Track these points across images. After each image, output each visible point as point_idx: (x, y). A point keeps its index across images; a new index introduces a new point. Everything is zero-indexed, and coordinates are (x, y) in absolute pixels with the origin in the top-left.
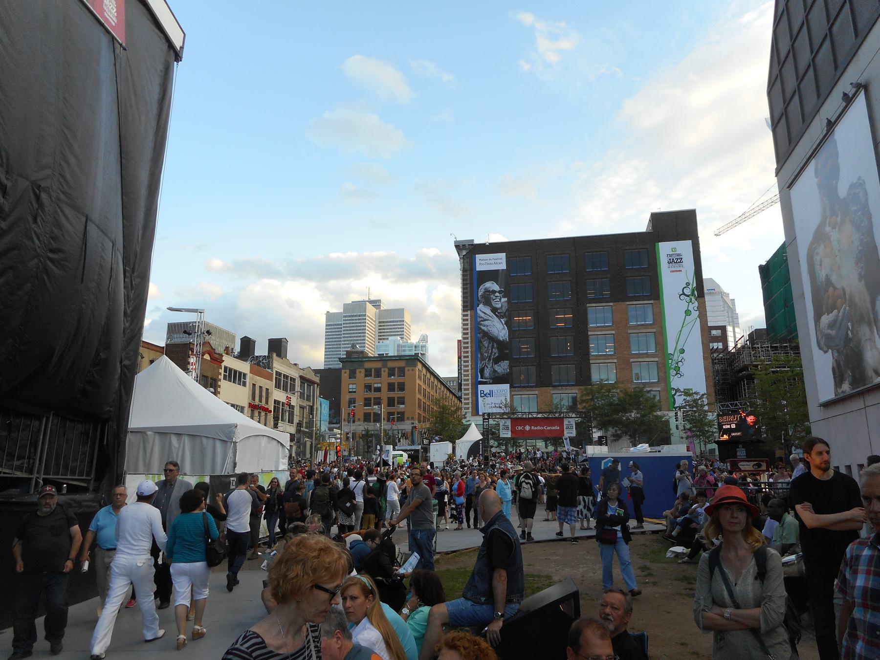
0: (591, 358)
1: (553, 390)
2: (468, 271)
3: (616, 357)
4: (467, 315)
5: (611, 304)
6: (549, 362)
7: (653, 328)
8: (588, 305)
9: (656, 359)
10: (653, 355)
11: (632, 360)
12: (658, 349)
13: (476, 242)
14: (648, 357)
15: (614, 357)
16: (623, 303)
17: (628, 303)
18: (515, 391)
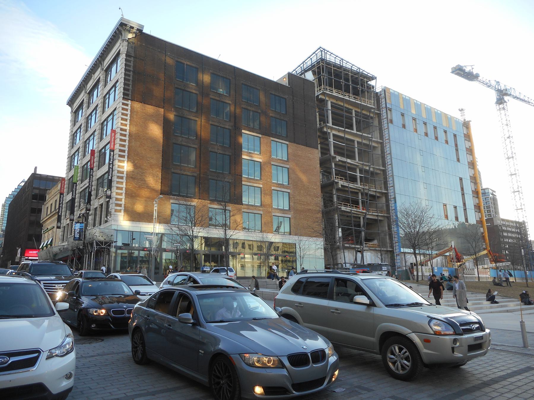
0: (243, 179)
1: (210, 204)
2: (132, 58)
3: (262, 183)
4: (127, 105)
5: (260, 136)
6: (208, 175)
7: (288, 164)
8: (243, 131)
9: (289, 191)
10: (286, 187)
11: (273, 188)
12: (290, 182)
13: (145, 31)
14: (283, 188)
15: (260, 182)
16: (268, 137)
17: (272, 138)
18: (174, 199)
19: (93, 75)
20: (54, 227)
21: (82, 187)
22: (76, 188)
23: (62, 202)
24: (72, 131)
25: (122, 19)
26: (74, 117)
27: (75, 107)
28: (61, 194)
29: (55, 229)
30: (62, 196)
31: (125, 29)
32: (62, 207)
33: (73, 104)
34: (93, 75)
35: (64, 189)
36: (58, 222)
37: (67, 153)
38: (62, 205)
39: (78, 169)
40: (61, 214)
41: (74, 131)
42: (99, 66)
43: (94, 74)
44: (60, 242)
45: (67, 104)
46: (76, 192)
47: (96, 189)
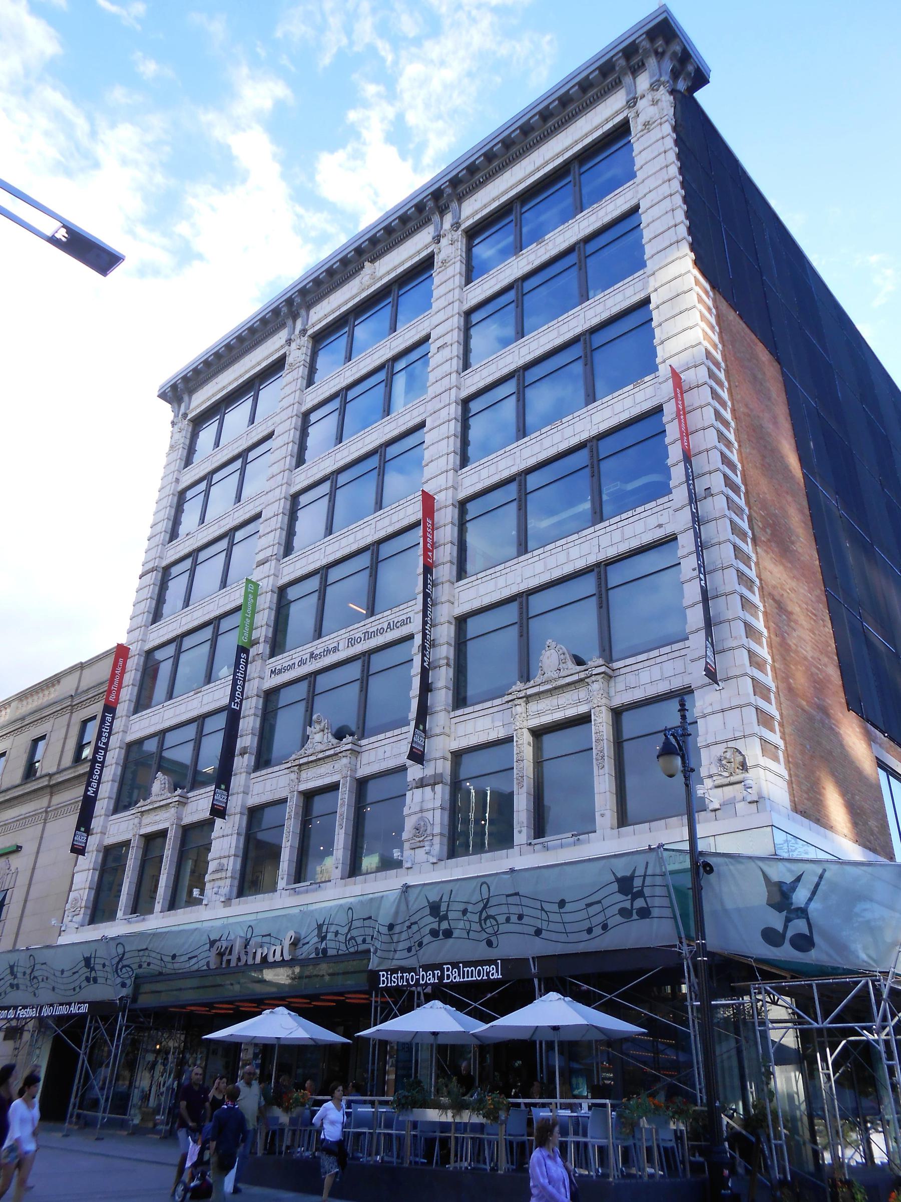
19: (367, 264)
20: (18, 849)
21: (280, 672)
22: (245, 671)
23: (107, 744)
24: (177, 480)
25: (664, 10)
26: (189, 436)
27: (198, 406)
28: (110, 708)
29: (16, 861)
30: (109, 718)
31: (663, 54)
32: (103, 763)
33: (191, 392)
34: (367, 264)
35: (120, 687)
36: (78, 829)
37: (142, 557)
38: (105, 756)
39: (256, 595)
40: (96, 792)
41: (186, 480)
42: (430, 220)
43: (372, 261)
44: (78, 919)
45: (163, 396)
46: (243, 687)
47: (452, 662)
